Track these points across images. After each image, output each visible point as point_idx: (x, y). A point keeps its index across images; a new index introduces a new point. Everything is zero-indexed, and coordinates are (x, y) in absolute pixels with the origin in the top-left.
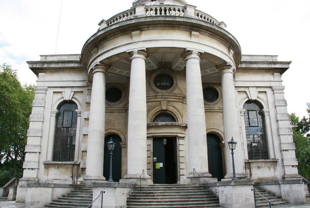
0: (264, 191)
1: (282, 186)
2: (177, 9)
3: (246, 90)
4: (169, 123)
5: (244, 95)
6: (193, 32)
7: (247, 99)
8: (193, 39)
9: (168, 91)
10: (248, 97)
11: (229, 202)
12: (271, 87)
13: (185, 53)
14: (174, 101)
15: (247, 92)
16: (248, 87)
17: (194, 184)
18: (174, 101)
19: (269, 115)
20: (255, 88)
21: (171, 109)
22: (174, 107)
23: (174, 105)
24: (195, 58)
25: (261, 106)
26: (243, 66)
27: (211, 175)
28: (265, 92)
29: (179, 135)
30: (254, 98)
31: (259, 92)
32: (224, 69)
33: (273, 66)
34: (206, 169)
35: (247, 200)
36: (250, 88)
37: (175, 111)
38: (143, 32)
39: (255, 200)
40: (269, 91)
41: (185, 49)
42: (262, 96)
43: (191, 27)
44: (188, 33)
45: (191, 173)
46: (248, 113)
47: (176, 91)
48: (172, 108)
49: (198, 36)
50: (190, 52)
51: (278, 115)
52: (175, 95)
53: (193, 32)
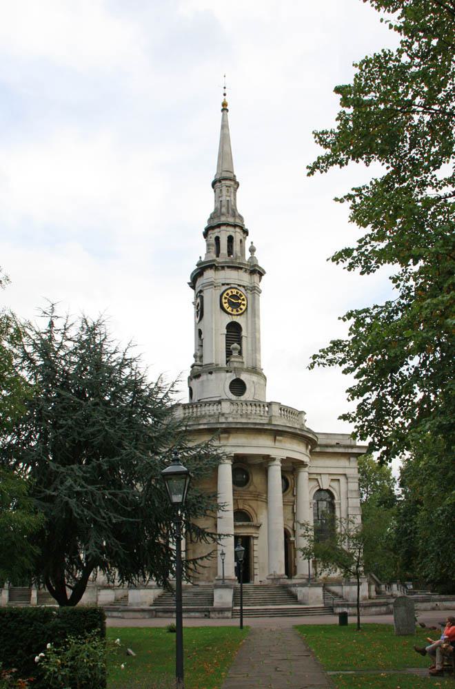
0: (329, 591)
1: (344, 587)
2: (262, 405)
3: (318, 477)
4: (245, 523)
5: (315, 483)
6: (277, 438)
7: (318, 488)
8: (278, 444)
9: (245, 487)
10: (319, 485)
11: (306, 598)
12: (345, 475)
13: (268, 459)
14: (249, 500)
15: (319, 480)
16: (320, 474)
17: (276, 584)
18: (249, 500)
19: (340, 508)
20: (327, 476)
21: (247, 508)
22: (250, 506)
23: (251, 504)
24: (277, 465)
25: (332, 497)
26: (318, 449)
27: (286, 577)
28: (339, 480)
29: (254, 535)
30: (325, 487)
31: (332, 480)
32: (300, 467)
33: (350, 451)
34: (283, 572)
35: (318, 597)
36: (322, 476)
37: (250, 510)
38: (231, 436)
39: (324, 598)
40: (342, 479)
41: (269, 455)
42: (335, 484)
43: (276, 433)
44: (272, 438)
45: (271, 575)
46: (318, 503)
47: (252, 488)
48: (248, 507)
49: (280, 441)
50: (274, 459)
51: (349, 509)
52: (251, 493)
53: (277, 438)
